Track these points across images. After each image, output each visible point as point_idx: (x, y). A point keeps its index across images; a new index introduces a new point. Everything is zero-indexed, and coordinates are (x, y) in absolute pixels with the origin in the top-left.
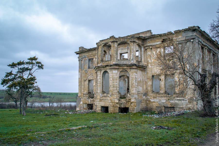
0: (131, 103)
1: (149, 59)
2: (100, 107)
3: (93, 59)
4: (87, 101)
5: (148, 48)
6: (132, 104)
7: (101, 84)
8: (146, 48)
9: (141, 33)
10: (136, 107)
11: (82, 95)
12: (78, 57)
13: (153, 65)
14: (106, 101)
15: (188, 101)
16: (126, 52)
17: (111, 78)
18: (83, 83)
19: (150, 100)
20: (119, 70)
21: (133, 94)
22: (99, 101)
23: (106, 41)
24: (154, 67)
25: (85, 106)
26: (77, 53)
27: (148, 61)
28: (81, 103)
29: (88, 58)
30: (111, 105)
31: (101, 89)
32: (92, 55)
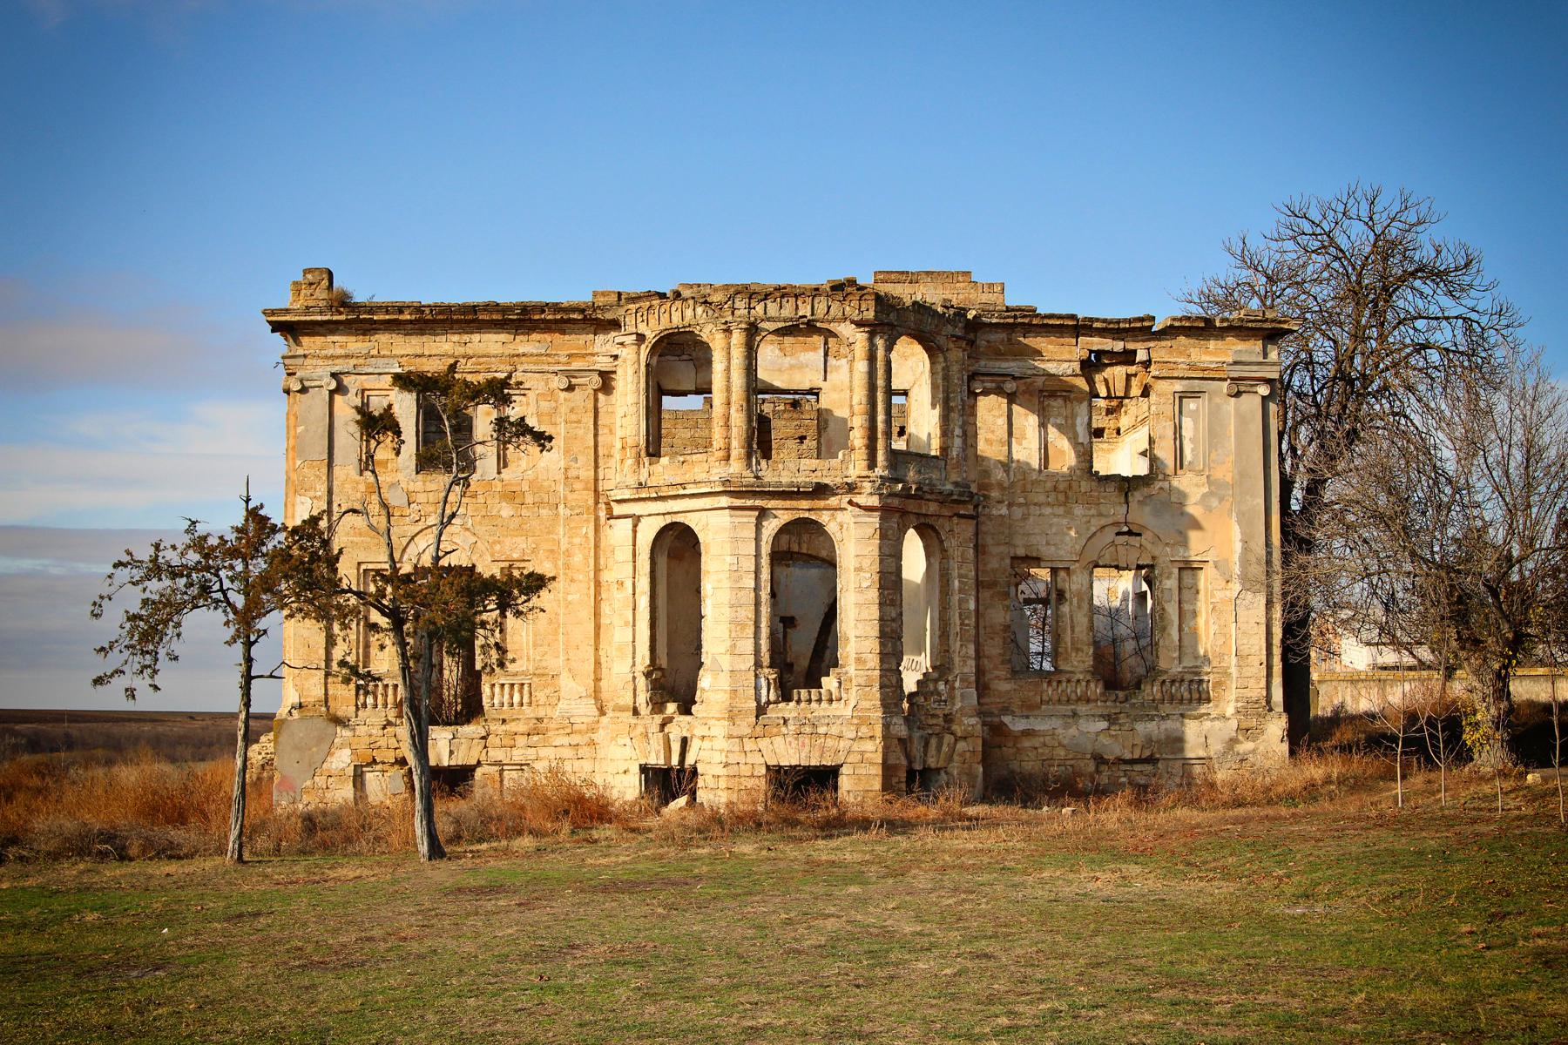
2: (763, 771)
5: (988, 385)
6: (961, 746)
9: (927, 273)
13: (1022, 500)
15: (1239, 721)
16: (807, 386)
19: (1007, 719)
23: (805, 310)
24: (1025, 518)
30: (862, 753)
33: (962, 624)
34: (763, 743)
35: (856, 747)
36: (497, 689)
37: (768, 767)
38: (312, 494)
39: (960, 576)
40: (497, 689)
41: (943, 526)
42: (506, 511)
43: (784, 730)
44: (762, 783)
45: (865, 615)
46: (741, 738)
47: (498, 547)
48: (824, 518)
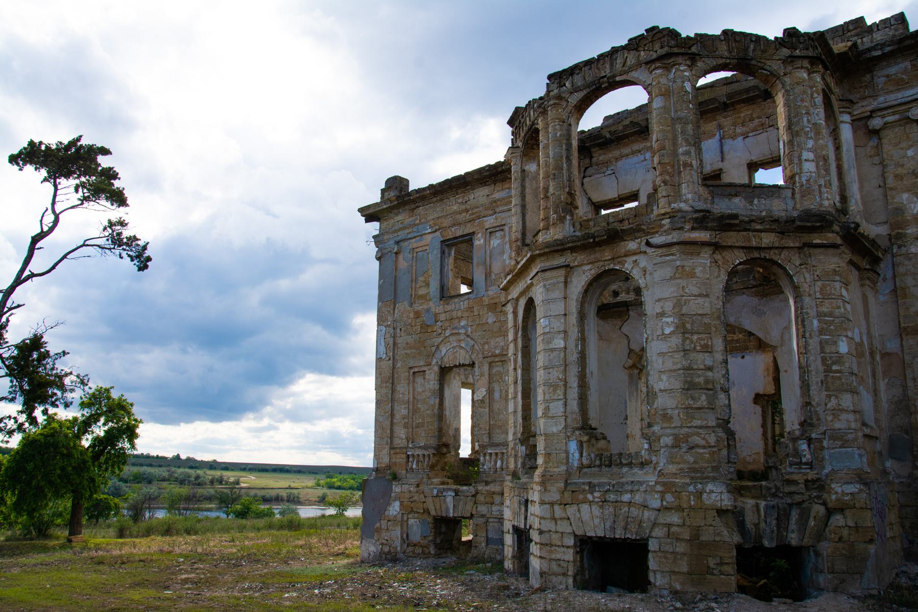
0: (830, 512)
1: (905, 196)
2: (570, 541)
3: (468, 239)
4: (429, 500)
5: (890, 119)
6: (838, 520)
7: (574, 371)
8: (876, 123)
10: (871, 541)
11: (400, 459)
12: (374, 237)
14: (626, 497)
17: (662, 314)
18: (402, 388)
20: (718, 256)
21: (838, 437)
22: (556, 497)
25: (417, 528)
26: (371, 211)
27: (899, 210)
28: (395, 509)
29: (438, 233)
30: (669, 525)
31: (574, 405)
32: (462, 217)
33: (828, 370)
34: (571, 510)
35: (661, 520)
36: (487, 458)
37: (575, 536)
38: (385, 324)
39: (819, 315)
40: (487, 458)
41: (791, 262)
42: (491, 318)
43: (590, 497)
44: (569, 555)
45: (669, 365)
46: (552, 504)
47: (486, 347)
48: (628, 266)
